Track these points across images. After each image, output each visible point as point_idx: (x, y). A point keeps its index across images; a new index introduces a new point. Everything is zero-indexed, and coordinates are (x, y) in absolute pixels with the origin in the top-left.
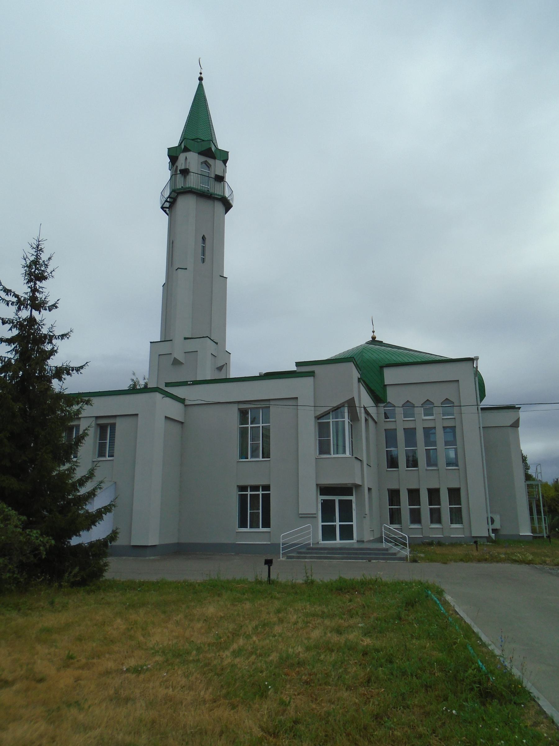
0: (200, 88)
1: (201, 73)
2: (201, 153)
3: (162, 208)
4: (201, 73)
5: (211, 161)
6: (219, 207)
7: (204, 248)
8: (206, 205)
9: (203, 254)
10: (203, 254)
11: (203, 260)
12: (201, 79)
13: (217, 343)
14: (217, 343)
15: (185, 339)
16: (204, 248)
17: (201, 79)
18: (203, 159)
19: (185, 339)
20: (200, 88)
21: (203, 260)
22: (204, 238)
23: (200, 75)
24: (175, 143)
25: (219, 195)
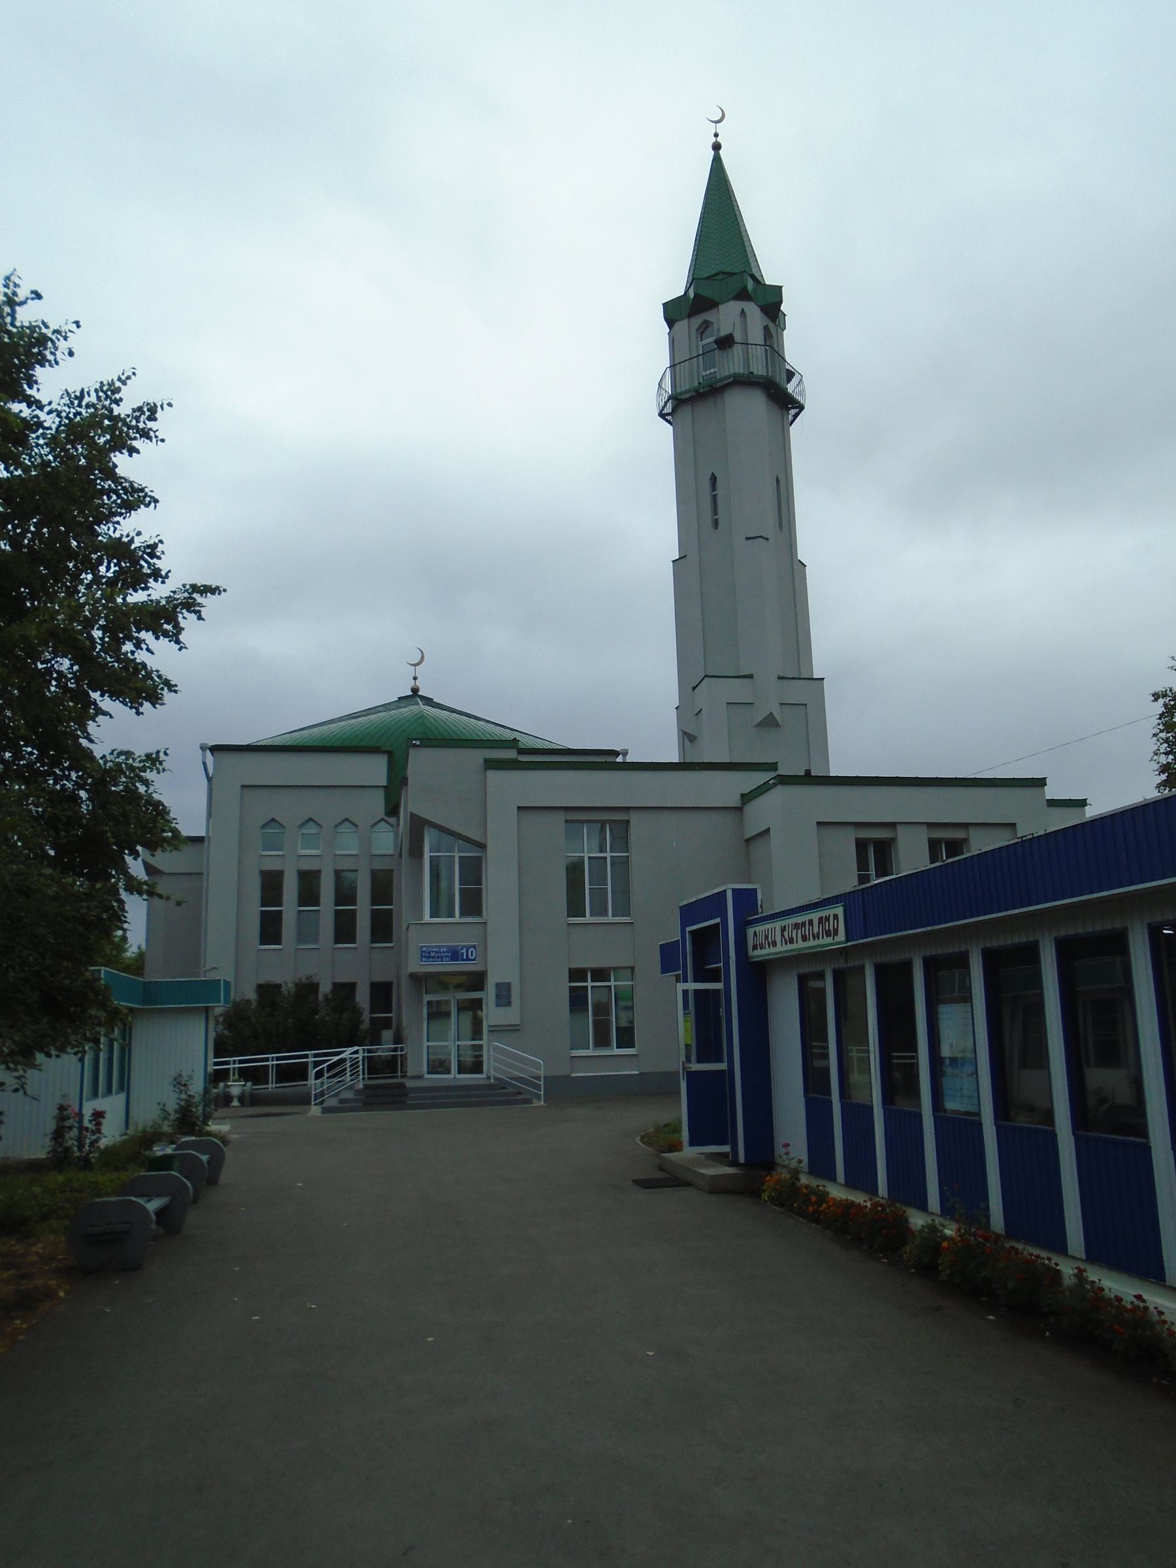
0: (717, 163)
1: (716, 135)
2: (691, 315)
4: (716, 135)
5: (708, 316)
7: (714, 498)
9: (715, 511)
10: (715, 511)
11: (716, 524)
12: (717, 147)
13: (750, 676)
14: (750, 676)
15: (694, 688)
16: (714, 498)
17: (717, 147)
18: (697, 321)
19: (694, 688)
20: (717, 163)
21: (716, 524)
22: (714, 479)
23: (714, 140)
25: (729, 377)
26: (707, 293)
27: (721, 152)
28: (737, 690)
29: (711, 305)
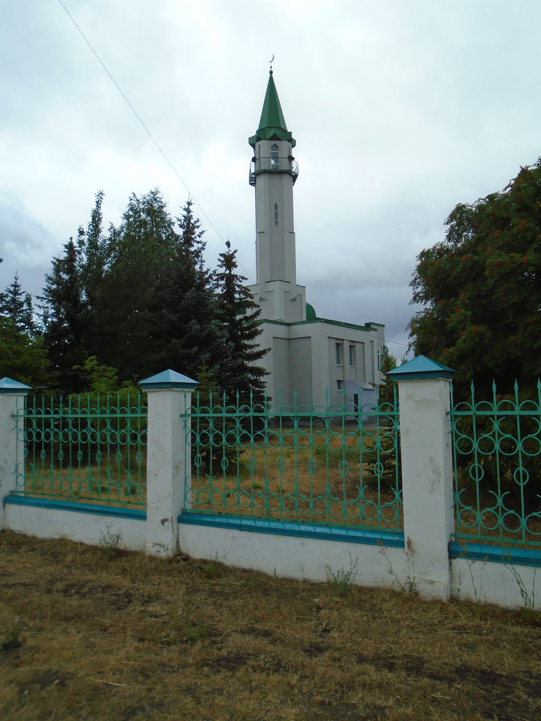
1: (271, 67)
3: (250, 184)
4: (271, 67)
5: (277, 143)
6: (287, 179)
7: (276, 214)
8: (276, 179)
11: (276, 223)
12: (271, 72)
13: (289, 282)
14: (289, 282)
15: (267, 282)
16: (276, 214)
17: (271, 72)
18: (272, 143)
19: (267, 282)
21: (276, 223)
23: (270, 69)
24: (254, 133)
26: (278, 134)
27: (273, 74)
28: (286, 287)
29: (279, 139)
